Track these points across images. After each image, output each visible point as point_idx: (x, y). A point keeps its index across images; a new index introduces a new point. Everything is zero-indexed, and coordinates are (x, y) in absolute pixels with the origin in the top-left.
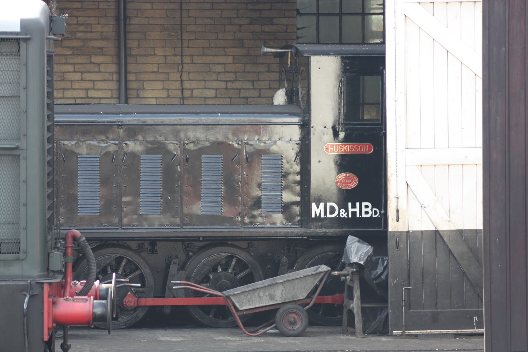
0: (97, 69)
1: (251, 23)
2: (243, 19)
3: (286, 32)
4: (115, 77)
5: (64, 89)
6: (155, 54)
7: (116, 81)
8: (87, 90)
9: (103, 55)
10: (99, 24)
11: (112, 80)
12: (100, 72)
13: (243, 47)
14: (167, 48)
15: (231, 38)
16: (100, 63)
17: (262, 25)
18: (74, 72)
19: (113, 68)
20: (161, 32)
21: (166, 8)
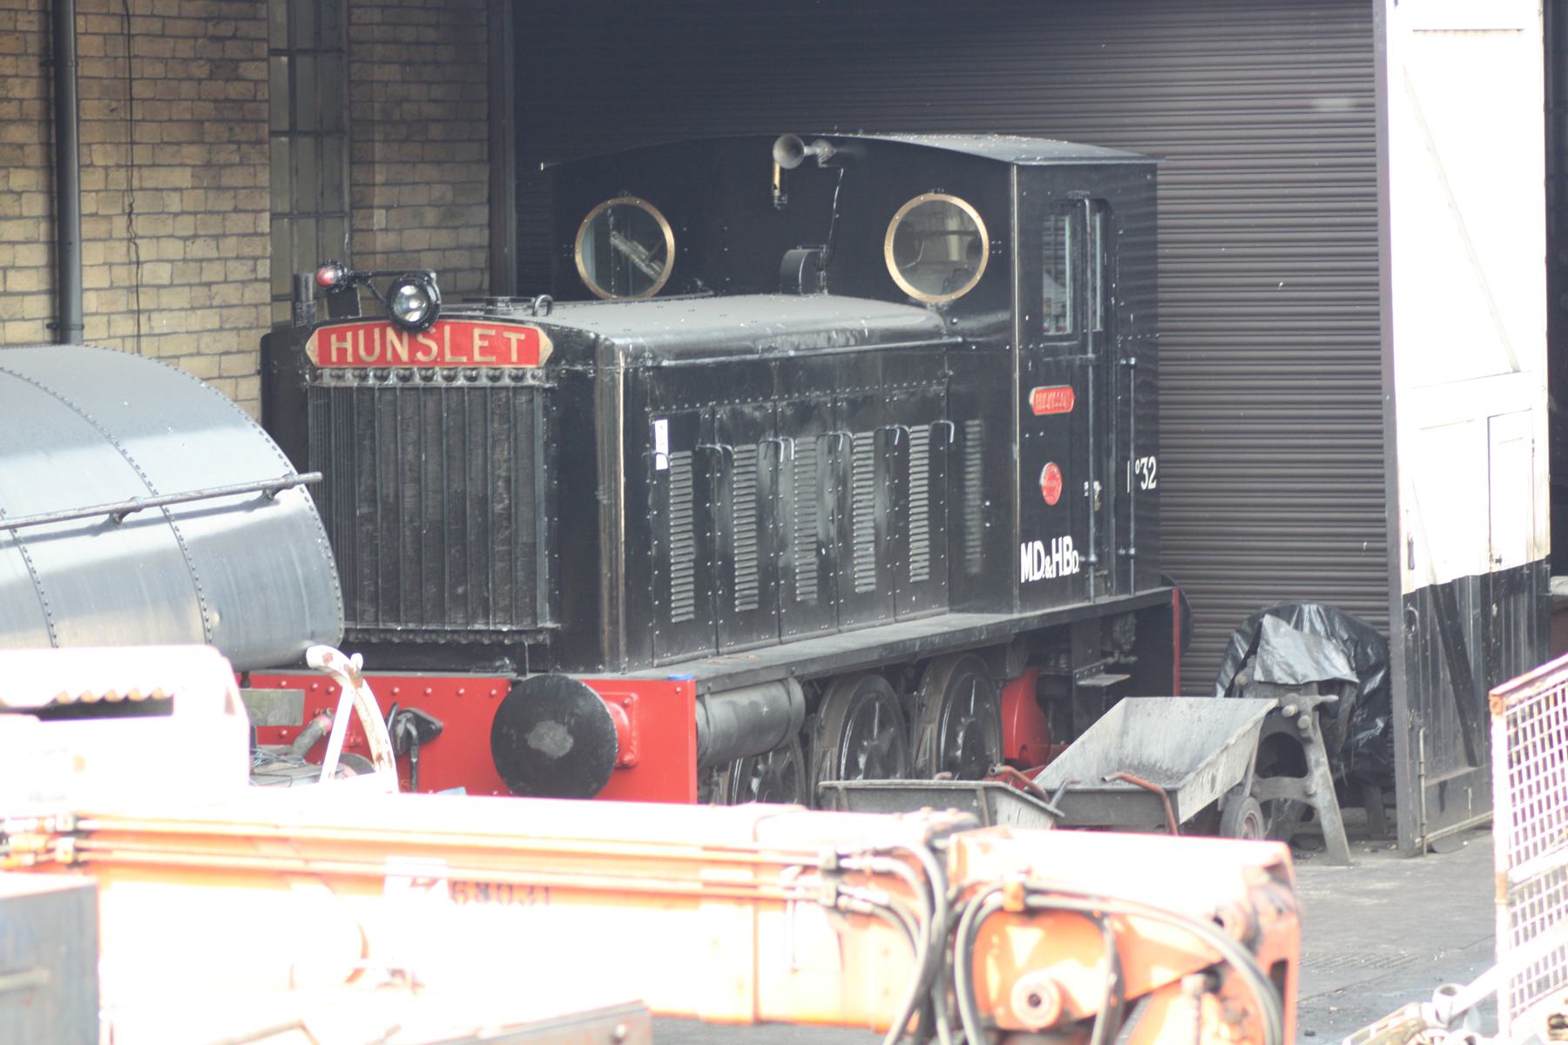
0: (17, 211)
1: (211, 77)
2: (202, 62)
3: (255, 100)
4: (42, 230)
6: (91, 165)
7: (44, 243)
9: (24, 167)
10: (16, 76)
11: (37, 242)
12: (21, 217)
13: (202, 142)
14: (109, 147)
15: (188, 116)
16: (19, 190)
17: (227, 80)
19: (36, 205)
20: (99, 99)
21: (105, 30)
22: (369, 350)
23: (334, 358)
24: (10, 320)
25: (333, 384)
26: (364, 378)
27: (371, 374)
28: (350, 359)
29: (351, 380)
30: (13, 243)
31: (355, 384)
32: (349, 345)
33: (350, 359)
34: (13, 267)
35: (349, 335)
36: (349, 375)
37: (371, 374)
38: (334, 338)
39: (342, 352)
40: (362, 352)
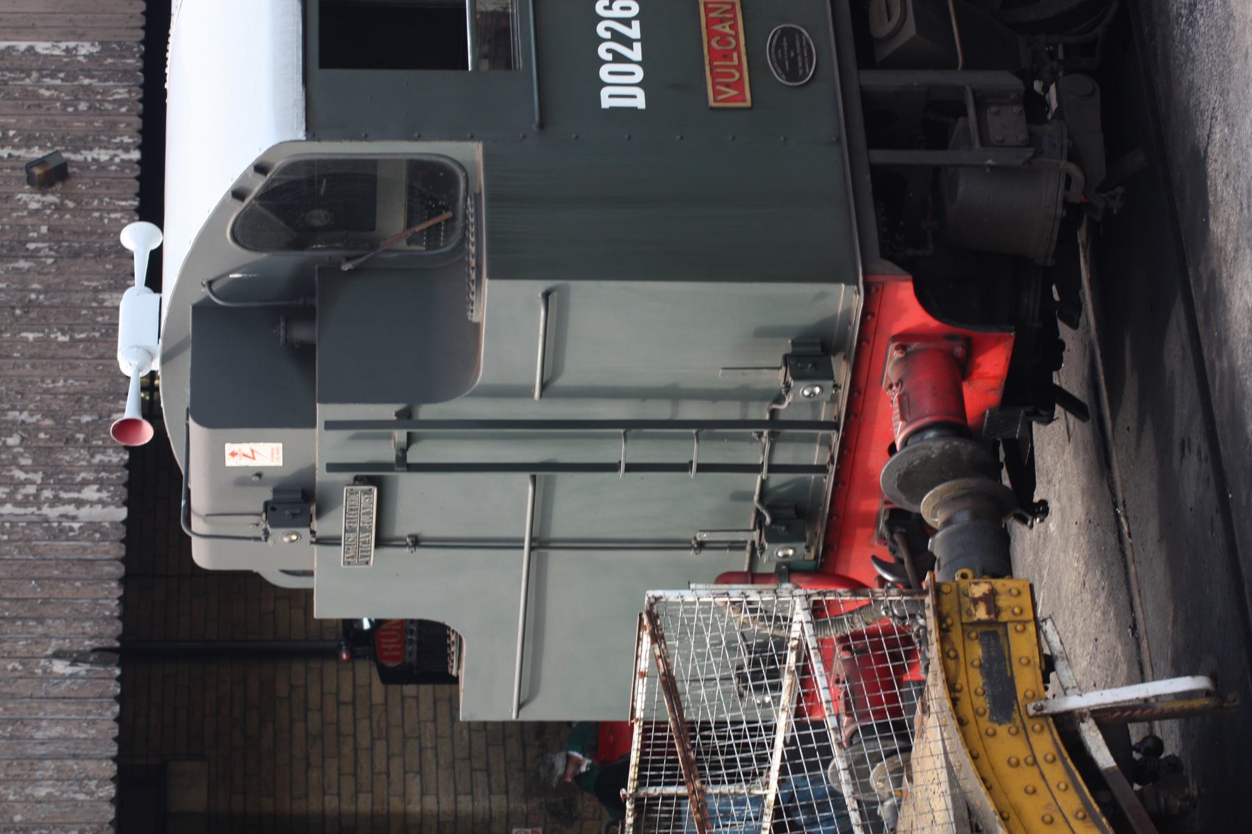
5: (339, 734)
8: (339, 703)
18: (306, 719)
22: (393, 637)
23: (398, 653)
24: (371, 700)
25: (414, 657)
26: (411, 641)
27: (409, 637)
28: (399, 646)
29: (413, 648)
30: (322, 694)
31: (416, 646)
32: (390, 647)
33: (399, 646)
34: (337, 694)
35: (384, 646)
36: (409, 648)
37: (409, 637)
38: (386, 654)
39: (394, 650)
40: (394, 640)
